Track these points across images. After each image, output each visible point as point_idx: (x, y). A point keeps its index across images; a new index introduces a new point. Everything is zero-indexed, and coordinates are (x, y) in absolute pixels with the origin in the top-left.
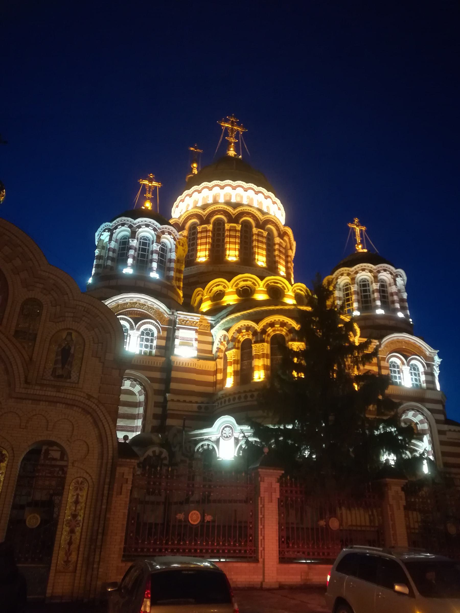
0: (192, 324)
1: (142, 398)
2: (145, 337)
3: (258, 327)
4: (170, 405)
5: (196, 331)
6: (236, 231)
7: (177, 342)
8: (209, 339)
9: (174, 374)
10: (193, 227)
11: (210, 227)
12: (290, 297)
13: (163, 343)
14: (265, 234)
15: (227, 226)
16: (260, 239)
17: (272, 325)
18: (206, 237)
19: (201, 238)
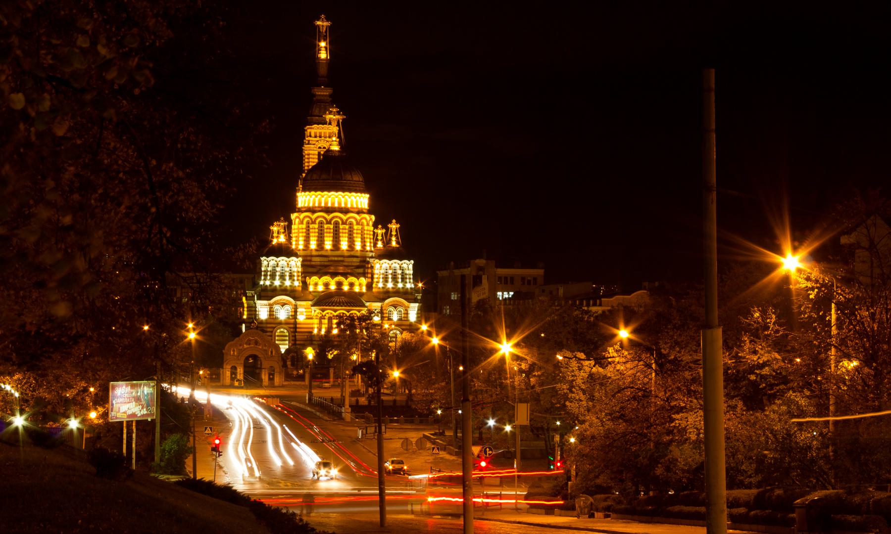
0: (304, 306)
1: (287, 334)
2: (287, 311)
3: (324, 314)
4: (297, 337)
5: (305, 308)
6: (330, 229)
7: (298, 313)
8: (310, 310)
9: (298, 326)
10: (308, 223)
11: (316, 226)
12: (346, 285)
13: (293, 314)
14: (347, 227)
15: (326, 226)
16: (344, 231)
17: (328, 313)
18: (315, 232)
19: (312, 232)
